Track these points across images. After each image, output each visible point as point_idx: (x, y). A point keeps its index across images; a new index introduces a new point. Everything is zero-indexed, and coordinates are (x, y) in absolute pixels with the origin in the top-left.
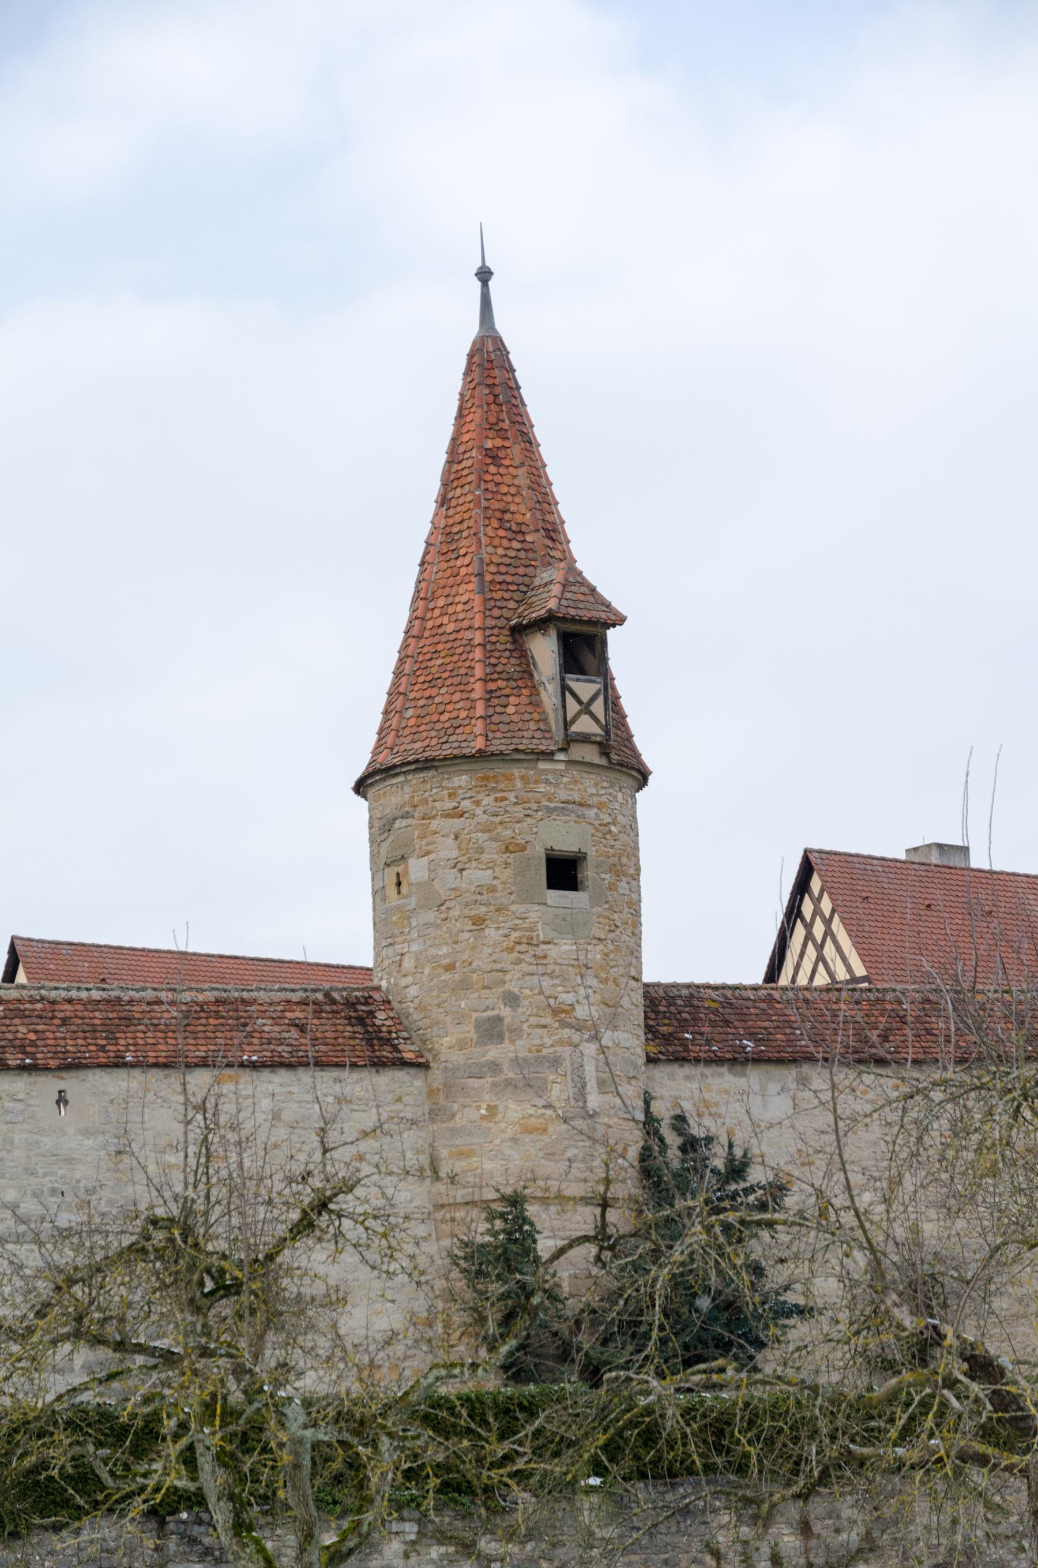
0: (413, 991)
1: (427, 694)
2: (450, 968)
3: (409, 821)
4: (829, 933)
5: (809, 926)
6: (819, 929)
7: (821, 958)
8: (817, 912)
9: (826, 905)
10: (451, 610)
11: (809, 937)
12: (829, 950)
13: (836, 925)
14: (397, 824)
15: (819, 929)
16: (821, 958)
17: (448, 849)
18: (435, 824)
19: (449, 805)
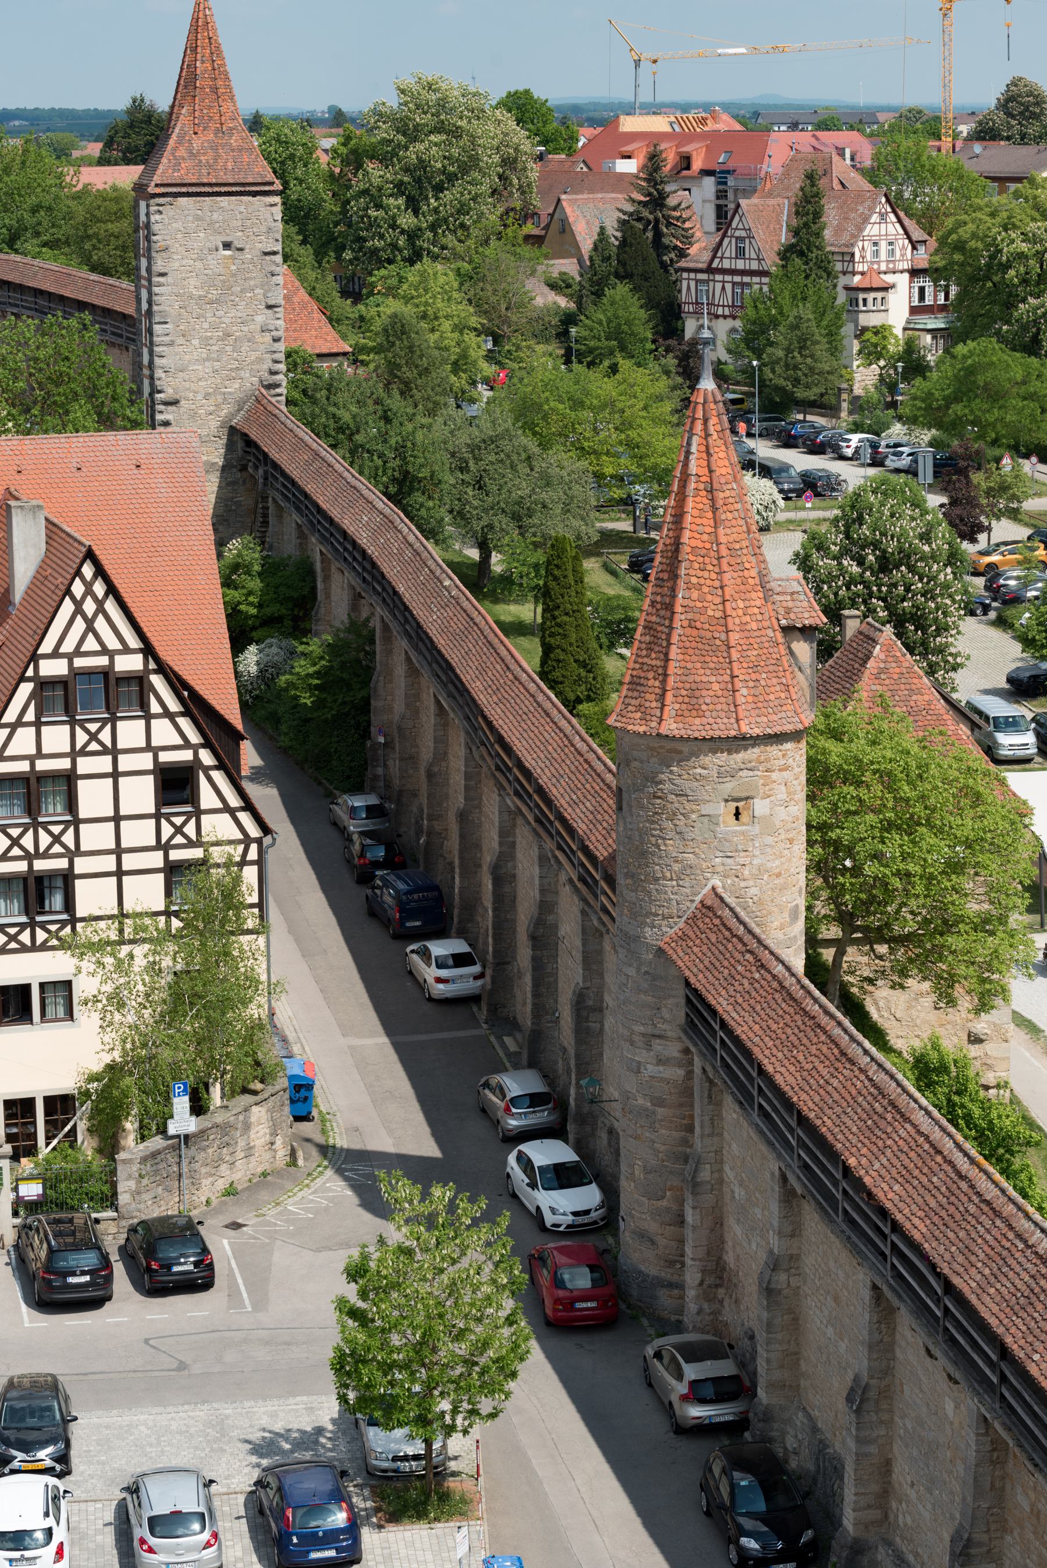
0: (753, 891)
1: (754, 677)
2: (778, 875)
3: (756, 773)
4: (101, 609)
5: (78, 604)
6: (89, 607)
7: (90, 628)
8: (89, 591)
9: (99, 588)
10: (750, 611)
11: (79, 610)
12: (100, 624)
13: (110, 606)
14: (745, 773)
15: (89, 607)
16: (90, 628)
17: (781, 793)
18: (774, 776)
19: (783, 762)
